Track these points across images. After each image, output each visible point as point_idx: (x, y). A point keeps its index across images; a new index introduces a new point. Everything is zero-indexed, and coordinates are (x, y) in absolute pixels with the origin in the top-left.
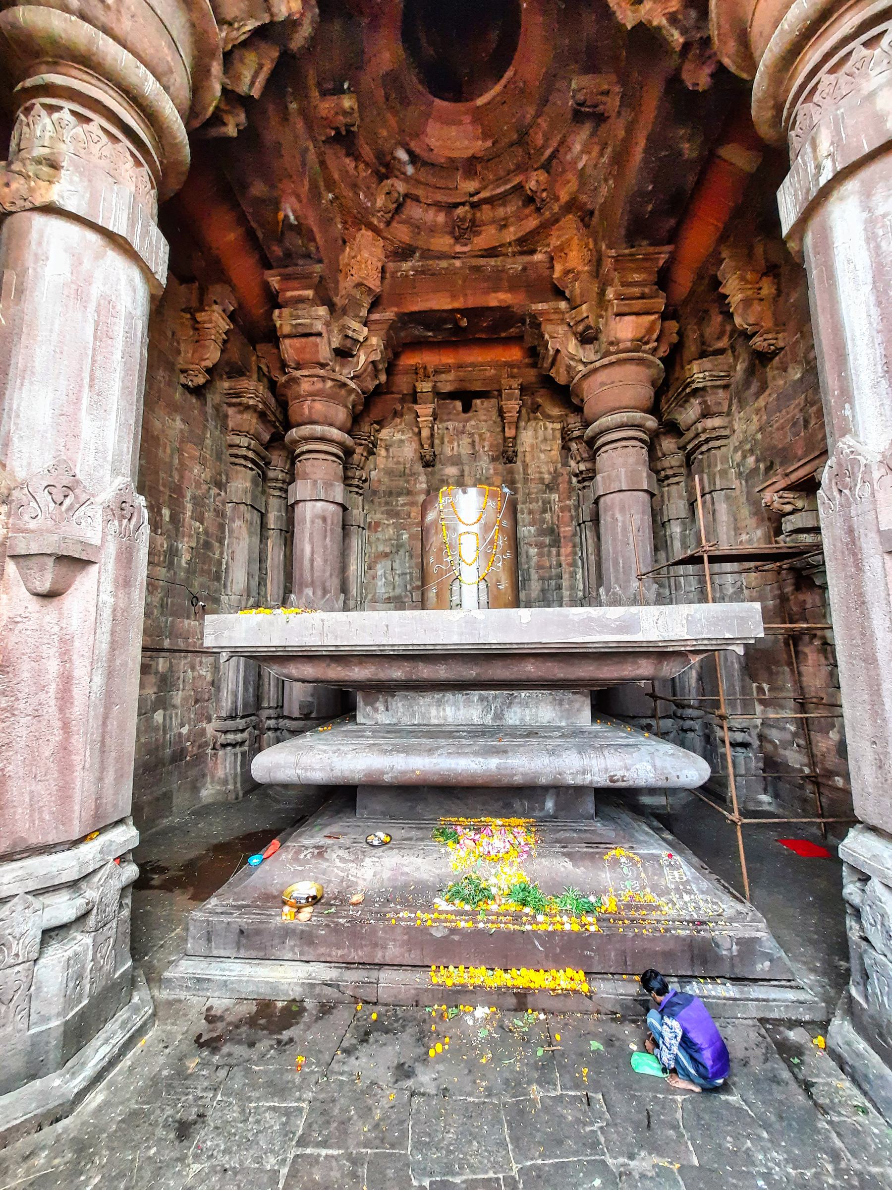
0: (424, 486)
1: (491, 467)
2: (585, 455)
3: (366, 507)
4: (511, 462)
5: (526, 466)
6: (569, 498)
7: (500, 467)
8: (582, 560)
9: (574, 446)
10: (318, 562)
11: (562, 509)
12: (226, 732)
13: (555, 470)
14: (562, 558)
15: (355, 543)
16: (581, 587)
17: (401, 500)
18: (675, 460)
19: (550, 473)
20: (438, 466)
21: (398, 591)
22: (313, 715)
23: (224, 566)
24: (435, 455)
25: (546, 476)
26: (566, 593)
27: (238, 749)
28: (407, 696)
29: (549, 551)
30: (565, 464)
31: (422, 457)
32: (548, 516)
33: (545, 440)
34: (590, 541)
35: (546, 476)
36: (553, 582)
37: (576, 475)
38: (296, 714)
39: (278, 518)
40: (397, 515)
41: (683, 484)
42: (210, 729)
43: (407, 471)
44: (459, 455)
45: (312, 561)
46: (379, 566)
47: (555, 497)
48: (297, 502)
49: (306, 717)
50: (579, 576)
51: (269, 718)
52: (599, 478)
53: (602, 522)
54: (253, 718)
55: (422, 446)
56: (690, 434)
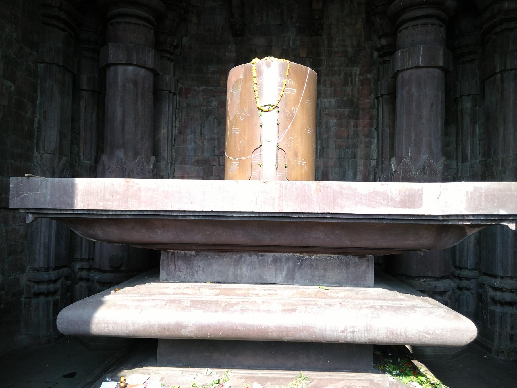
0: (234, 55)
6: (370, 72)
8: (377, 129)
11: (362, 83)
12: (39, 282)
14: (360, 129)
15: (166, 108)
16: (375, 157)
17: (211, 68)
21: (206, 155)
22: (123, 268)
23: (36, 125)
25: (349, 49)
26: (361, 162)
27: (51, 299)
28: (207, 256)
29: (348, 123)
32: (348, 89)
35: (349, 49)
36: (349, 152)
37: (378, 50)
38: (107, 267)
42: (24, 279)
46: (188, 131)
47: (357, 70)
48: (109, 65)
49: (115, 269)
50: (374, 146)
51: (82, 269)
52: (399, 54)
53: (399, 96)
54: (66, 270)
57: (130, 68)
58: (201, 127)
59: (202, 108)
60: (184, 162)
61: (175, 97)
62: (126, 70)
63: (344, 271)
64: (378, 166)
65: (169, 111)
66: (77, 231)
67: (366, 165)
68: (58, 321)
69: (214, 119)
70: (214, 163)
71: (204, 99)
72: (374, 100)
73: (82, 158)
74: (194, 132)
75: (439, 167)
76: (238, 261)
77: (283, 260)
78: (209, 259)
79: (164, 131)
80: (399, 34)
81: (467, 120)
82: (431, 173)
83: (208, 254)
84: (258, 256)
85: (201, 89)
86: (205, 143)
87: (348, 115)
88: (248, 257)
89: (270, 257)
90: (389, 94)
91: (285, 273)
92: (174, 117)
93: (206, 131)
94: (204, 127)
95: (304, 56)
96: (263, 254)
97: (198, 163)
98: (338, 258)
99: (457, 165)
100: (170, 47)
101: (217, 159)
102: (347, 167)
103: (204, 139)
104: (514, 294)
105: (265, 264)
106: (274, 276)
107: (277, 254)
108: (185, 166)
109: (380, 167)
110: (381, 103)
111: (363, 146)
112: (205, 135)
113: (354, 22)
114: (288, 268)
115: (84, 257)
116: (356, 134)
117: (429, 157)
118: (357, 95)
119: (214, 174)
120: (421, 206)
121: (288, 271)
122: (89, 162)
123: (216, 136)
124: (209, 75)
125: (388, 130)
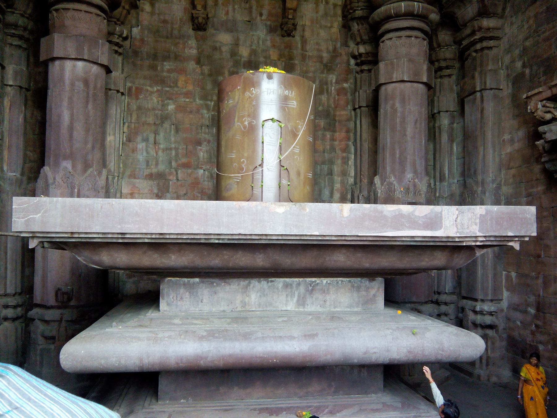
0: (194, 52)
1: (269, 38)
2: (365, 37)
3: (126, 70)
4: (289, 35)
5: (304, 41)
6: (346, 81)
7: (278, 39)
9: (355, 27)
10: (79, 128)
13: (335, 50)
15: (115, 111)
16: (352, 173)
17: (167, 65)
18: (448, 53)
19: (328, 51)
20: (211, 31)
22: (72, 303)
24: (208, 18)
26: (337, 179)
28: (213, 283)
29: (324, 136)
30: (346, 44)
31: (193, 19)
32: (324, 98)
33: (326, 15)
34: (365, 127)
35: (325, 55)
36: (326, 167)
37: (354, 57)
39: (16, 73)
40: (162, 82)
41: (454, 77)
43: (176, 32)
44: (234, 22)
45: (71, 128)
46: (139, 138)
47: (333, 78)
48: (54, 59)
52: (381, 65)
53: (382, 111)
55: (194, 7)
56: (468, 31)
57: (80, 64)
58: (155, 134)
59: (157, 112)
60: (133, 176)
61: (124, 97)
62: (74, 66)
63: (355, 294)
64: (355, 183)
65: (116, 114)
66: (80, 257)
67: (342, 183)
68: (61, 356)
69: (171, 126)
70: (171, 177)
71: (158, 102)
72: (351, 112)
73: (5, 168)
74: (146, 140)
75: (423, 187)
76: (247, 288)
77: (294, 285)
78: (215, 286)
79: (110, 138)
80: (381, 44)
81: (445, 138)
82: (415, 193)
83: (214, 280)
84: (268, 282)
85: (155, 89)
86: (160, 153)
87: (324, 127)
88: (257, 283)
89: (280, 282)
90: (367, 106)
91: (295, 299)
92: (122, 121)
93: (161, 137)
94: (159, 134)
95: (276, 59)
96: (273, 279)
97: (150, 177)
98: (350, 281)
99: (435, 185)
100: (118, 38)
101: (175, 173)
102: (323, 185)
103: (159, 148)
104: (494, 317)
105: (275, 290)
106: (284, 302)
107: (288, 280)
108: (135, 180)
109: (358, 186)
110: (359, 115)
111: (339, 161)
112: (159, 144)
113: (329, 25)
114: (299, 294)
115: (8, 291)
116: (333, 149)
117: (414, 176)
118: (333, 106)
119: (170, 190)
120: (441, 228)
121: (299, 296)
122: (14, 174)
123: (173, 146)
124: (165, 74)
125: (366, 146)
